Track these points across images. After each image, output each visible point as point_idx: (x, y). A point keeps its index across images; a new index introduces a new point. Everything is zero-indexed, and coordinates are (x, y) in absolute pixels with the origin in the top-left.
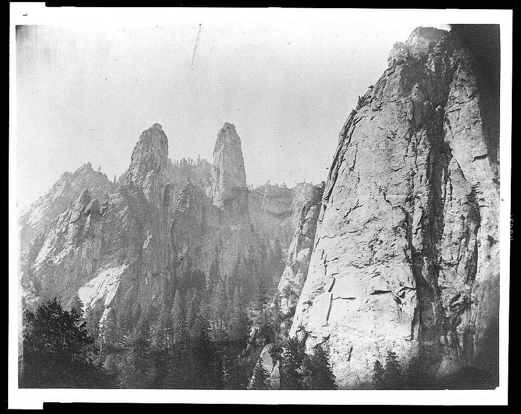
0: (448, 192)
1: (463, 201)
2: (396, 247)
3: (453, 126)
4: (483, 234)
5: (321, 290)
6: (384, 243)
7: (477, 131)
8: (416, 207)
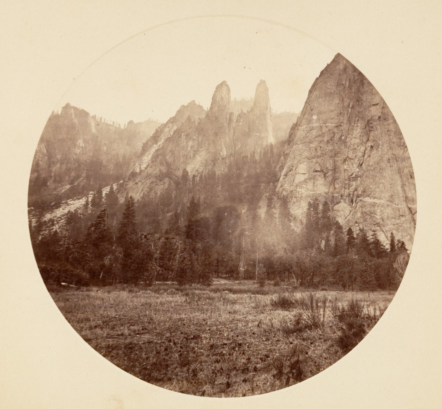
1: (362, 128)
2: (327, 150)
6: (322, 148)
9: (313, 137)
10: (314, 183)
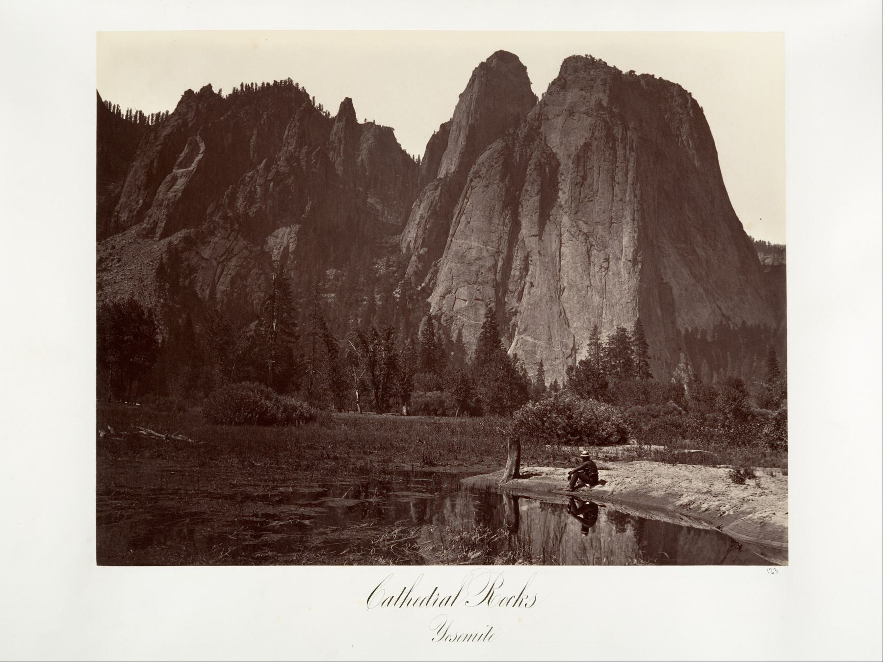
0: (516, 251)
1: (522, 259)
3: (524, 210)
4: (528, 279)
5: (449, 292)
7: (536, 218)
8: (500, 259)
9: (473, 258)
10: (476, 312)
